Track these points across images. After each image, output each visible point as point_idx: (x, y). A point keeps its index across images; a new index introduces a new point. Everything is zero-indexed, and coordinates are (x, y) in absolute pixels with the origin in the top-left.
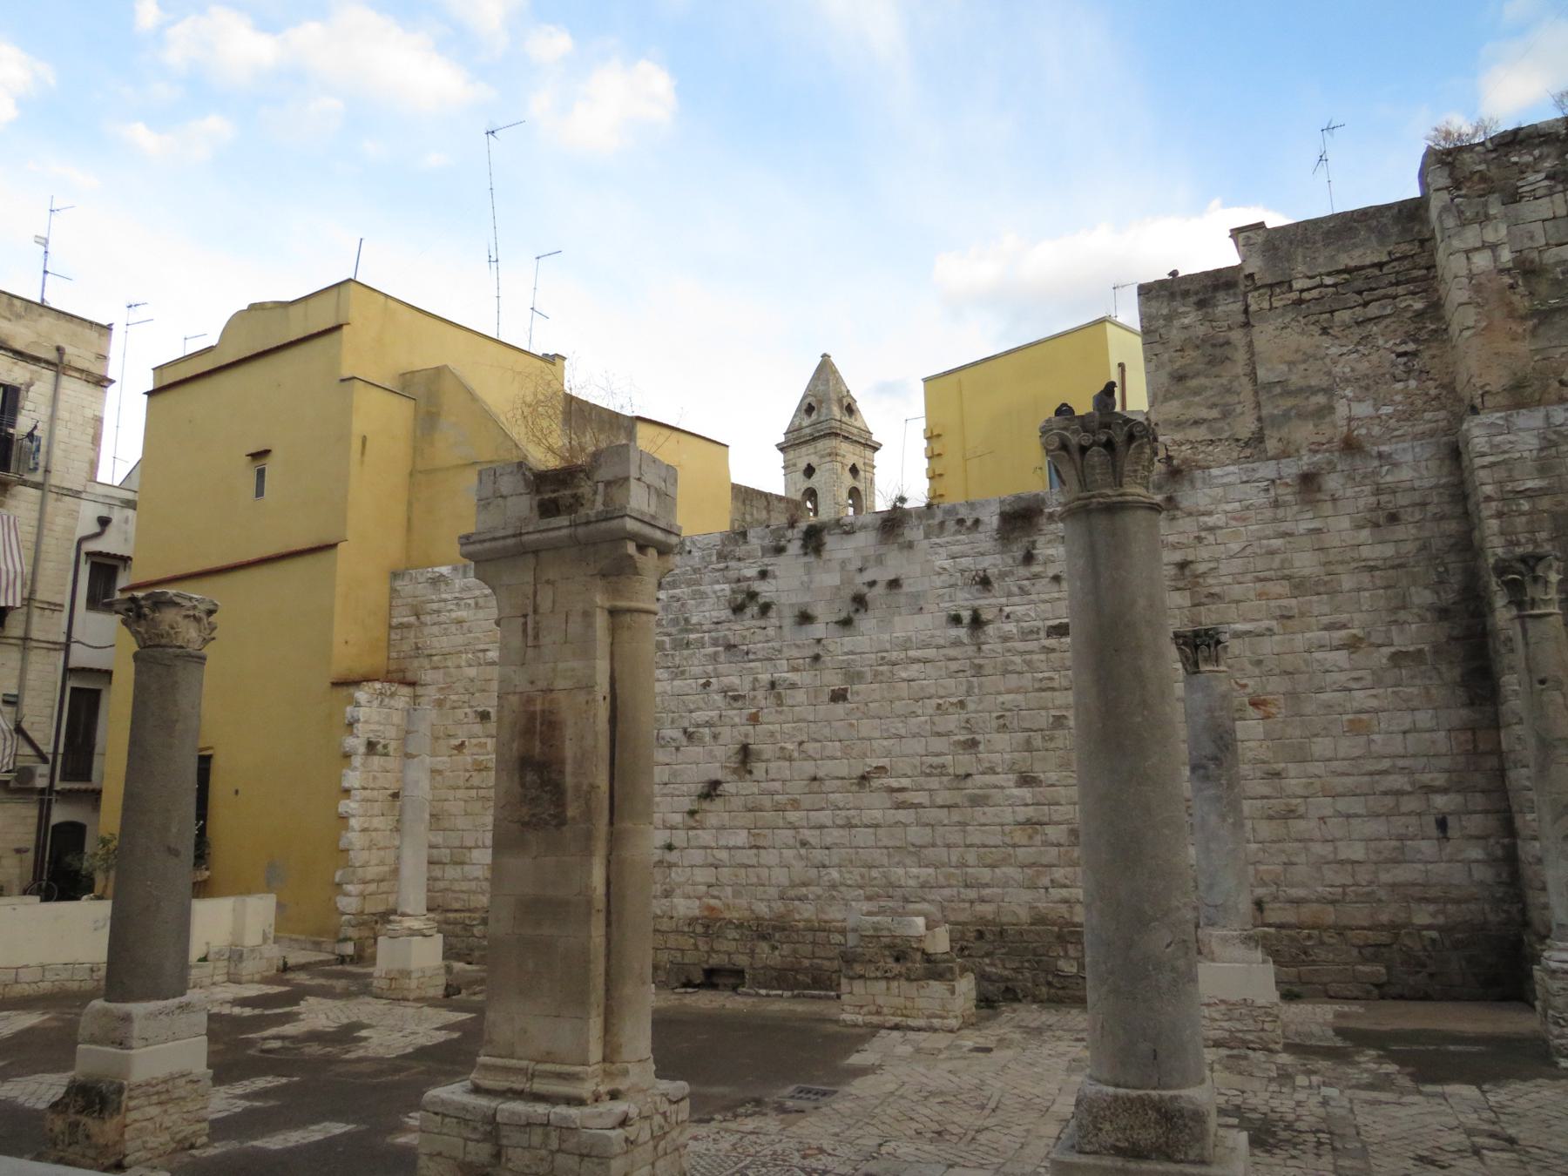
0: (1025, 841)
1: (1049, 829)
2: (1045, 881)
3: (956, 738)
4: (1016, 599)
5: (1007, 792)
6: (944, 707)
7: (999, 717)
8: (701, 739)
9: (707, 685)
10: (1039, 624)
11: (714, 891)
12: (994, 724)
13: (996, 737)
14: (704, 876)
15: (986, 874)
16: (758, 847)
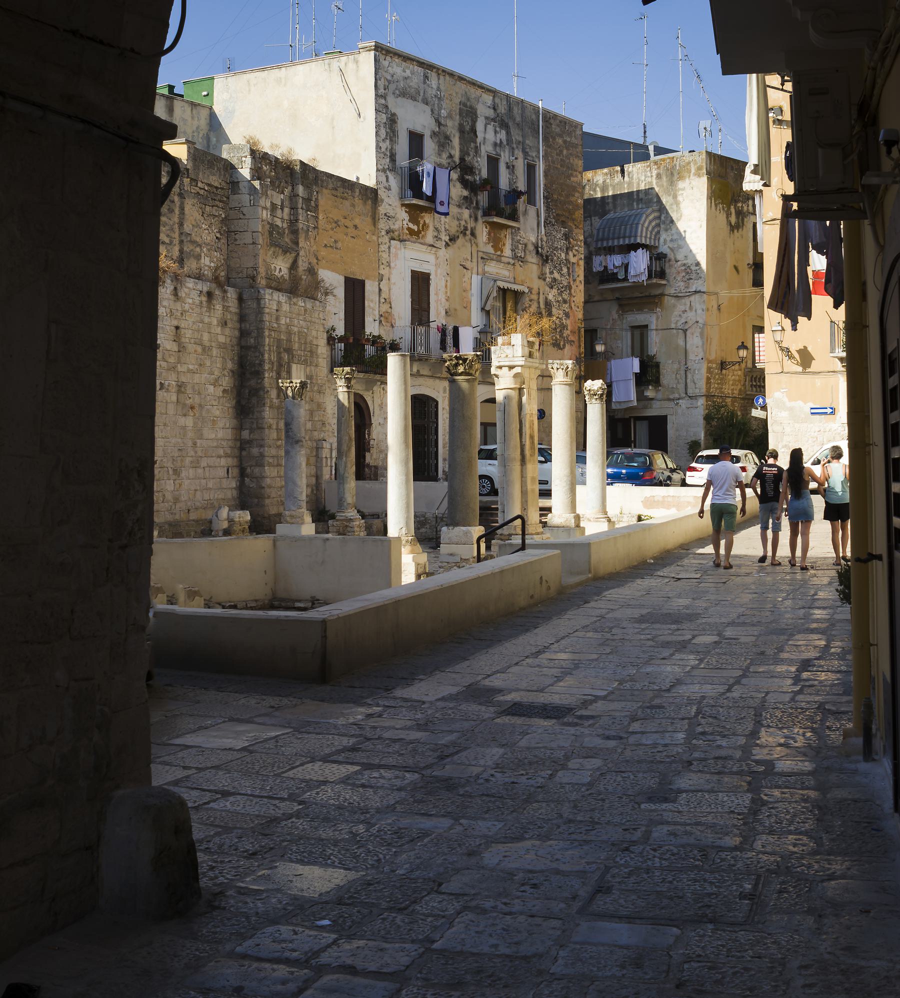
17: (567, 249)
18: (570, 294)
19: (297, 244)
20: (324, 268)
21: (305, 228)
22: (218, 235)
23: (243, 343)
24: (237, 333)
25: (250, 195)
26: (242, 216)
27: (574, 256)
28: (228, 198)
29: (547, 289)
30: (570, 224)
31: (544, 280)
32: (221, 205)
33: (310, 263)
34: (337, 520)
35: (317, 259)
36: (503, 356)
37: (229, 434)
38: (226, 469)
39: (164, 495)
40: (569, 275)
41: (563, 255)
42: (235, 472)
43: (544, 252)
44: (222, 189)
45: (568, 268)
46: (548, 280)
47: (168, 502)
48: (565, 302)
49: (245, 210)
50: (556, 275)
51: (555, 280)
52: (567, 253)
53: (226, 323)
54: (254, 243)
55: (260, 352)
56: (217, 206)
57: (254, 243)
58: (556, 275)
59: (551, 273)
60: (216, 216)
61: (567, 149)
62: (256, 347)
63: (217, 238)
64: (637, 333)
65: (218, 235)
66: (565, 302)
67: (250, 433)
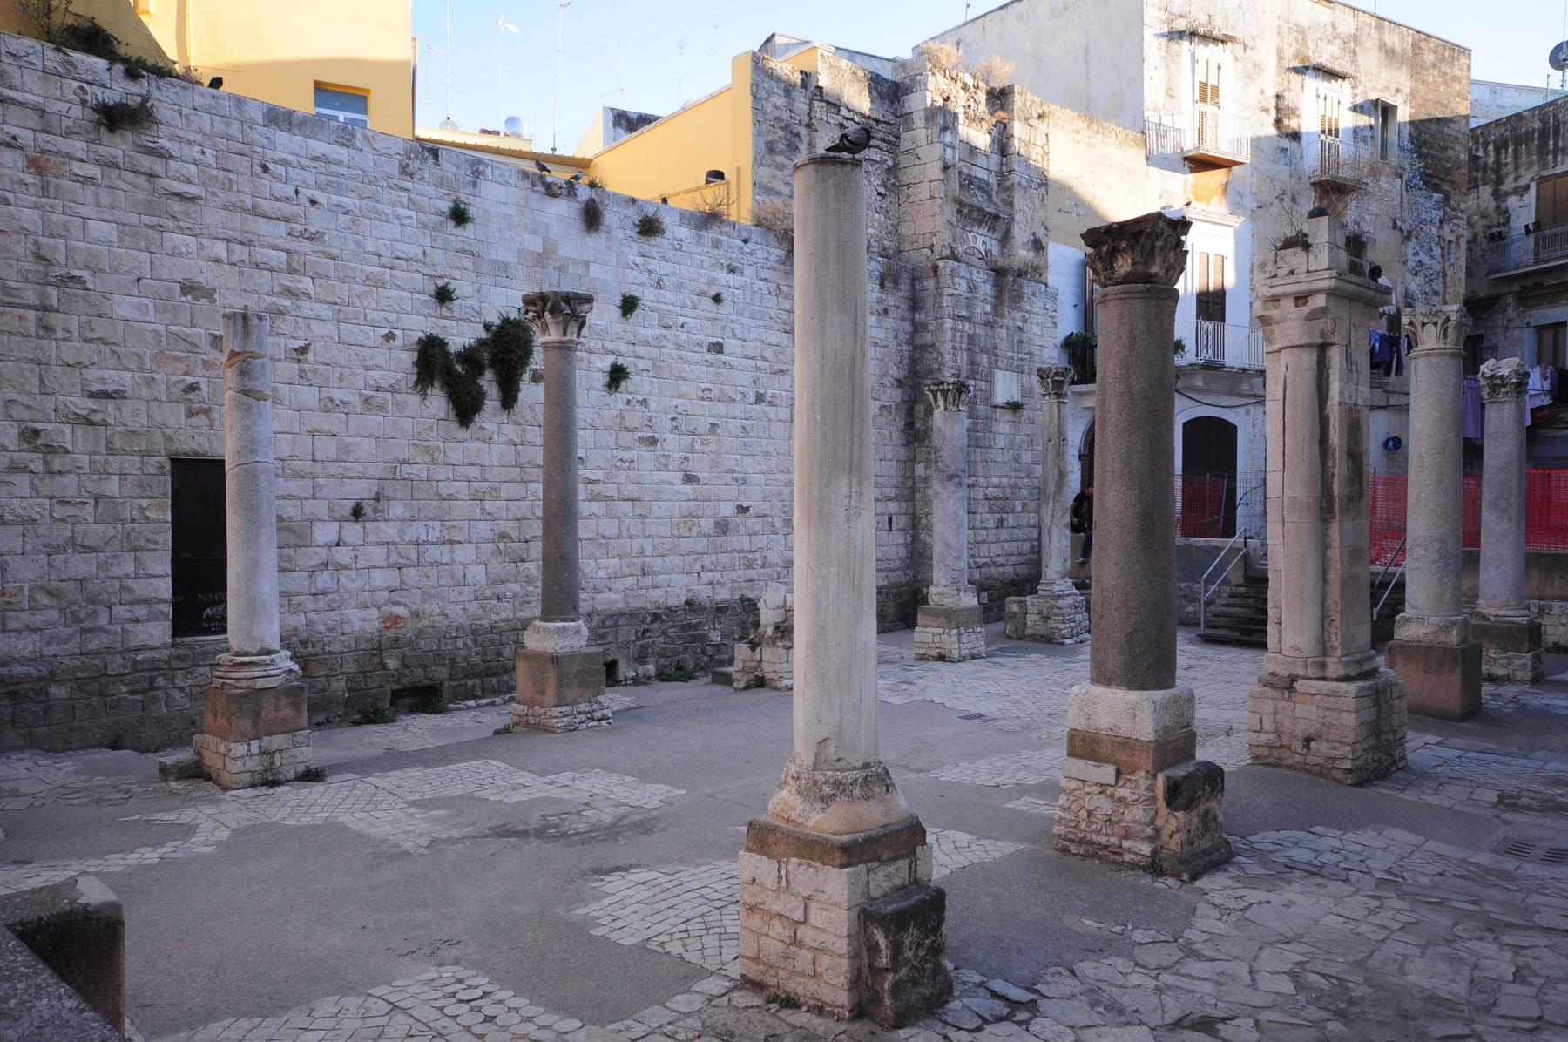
0: (686, 533)
1: (702, 522)
2: (698, 567)
3: (640, 435)
4: (688, 312)
5: (676, 487)
6: (633, 403)
7: (673, 419)
8: (382, 408)
9: (390, 337)
10: (703, 338)
11: (396, 596)
12: (669, 425)
13: (668, 436)
14: (381, 578)
15: (658, 563)
16: (452, 542)
17: (1441, 221)
18: (1445, 283)
19: (1011, 205)
20: (1054, 241)
21: (1024, 183)
22: (882, 190)
23: (918, 341)
24: (907, 326)
25: (926, 128)
26: (916, 162)
27: (1452, 231)
28: (898, 138)
29: (1409, 276)
30: (1447, 187)
31: (1405, 263)
32: (883, 145)
33: (1034, 234)
34: (1040, 597)
35: (1046, 228)
36: (1284, 271)
37: (890, 468)
38: (886, 518)
39: (765, 557)
40: (1443, 256)
41: (1434, 231)
42: (901, 521)
43: (1405, 227)
44: (887, 123)
45: (1442, 248)
46: (1409, 263)
47: (772, 566)
48: (1436, 294)
49: (920, 152)
50: (1423, 257)
51: (1420, 264)
52: (1441, 227)
53: (886, 311)
54: (932, 197)
55: (939, 352)
56: (878, 147)
57: (932, 197)
58: (1423, 257)
59: (1416, 254)
60: (876, 162)
61: (1445, 83)
62: (933, 346)
63: (879, 194)
64: (1548, 336)
65: (882, 190)
66: (1436, 294)
67: (926, 468)
